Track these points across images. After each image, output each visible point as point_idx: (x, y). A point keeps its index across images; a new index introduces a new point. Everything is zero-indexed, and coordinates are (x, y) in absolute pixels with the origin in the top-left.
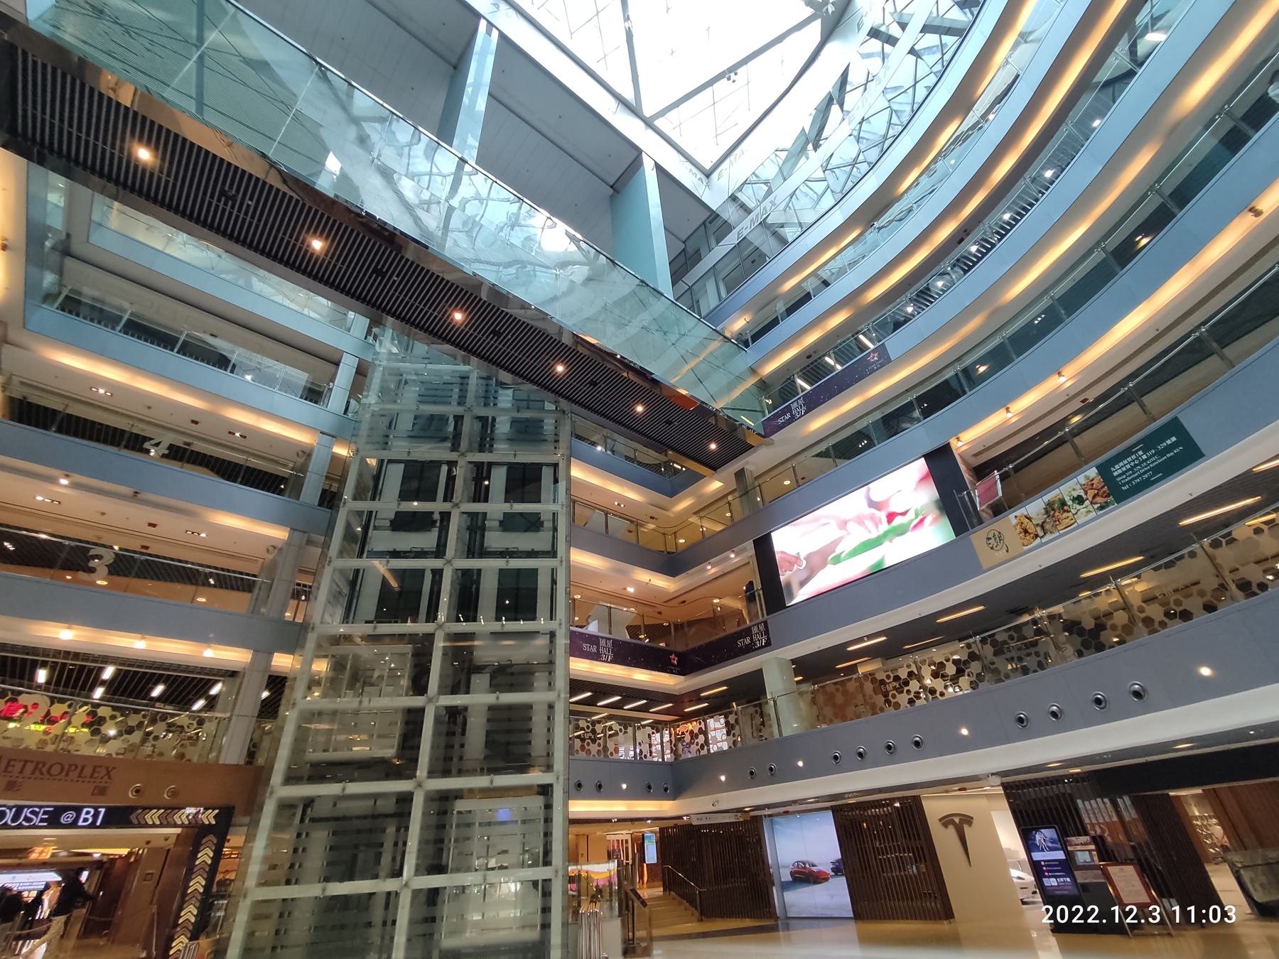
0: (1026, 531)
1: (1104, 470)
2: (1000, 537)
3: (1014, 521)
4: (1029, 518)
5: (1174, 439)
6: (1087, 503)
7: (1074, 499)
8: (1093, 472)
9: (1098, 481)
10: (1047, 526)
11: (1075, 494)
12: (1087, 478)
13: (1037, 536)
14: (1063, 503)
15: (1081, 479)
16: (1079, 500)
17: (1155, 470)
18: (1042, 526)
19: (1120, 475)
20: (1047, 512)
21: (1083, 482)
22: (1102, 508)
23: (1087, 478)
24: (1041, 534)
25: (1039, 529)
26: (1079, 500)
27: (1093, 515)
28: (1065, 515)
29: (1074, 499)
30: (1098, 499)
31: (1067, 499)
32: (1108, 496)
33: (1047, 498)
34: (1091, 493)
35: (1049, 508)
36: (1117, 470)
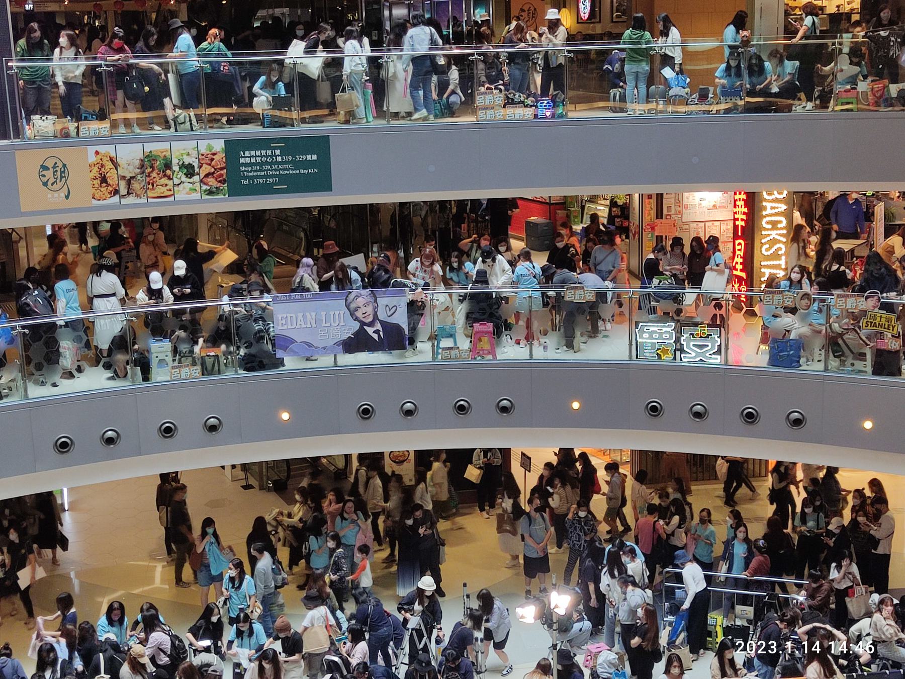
0: (104, 180)
1: (233, 147)
2: (62, 172)
3: (92, 159)
4: (116, 165)
5: (315, 157)
6: (196, 178)
7: (182, 166)
8: (219, 145)
9: (220, 157)
10: (136, 186)
11: (187, 160)
12: (210, 147)
13: (116, 192)
14: (168, 165)
15: (203, 146)
16: (189, 170)
17: (283, 179)
18: (129, 182)
19: (245, 165)
20: (142, 166)
21: (203, 150)
22: (210, 192)
23: (210, 147)
24: (123, 191)
25: (123, 184)
26: (189, 170)
27: (197, 196)
28: (164, 181)
29: (182, 166)
30: (212, 181)
31: (175, 161)
32: (223, 182)
33: (150, 147)
34: (206, 169)
35: (148, 163)
36: (247, 157)
